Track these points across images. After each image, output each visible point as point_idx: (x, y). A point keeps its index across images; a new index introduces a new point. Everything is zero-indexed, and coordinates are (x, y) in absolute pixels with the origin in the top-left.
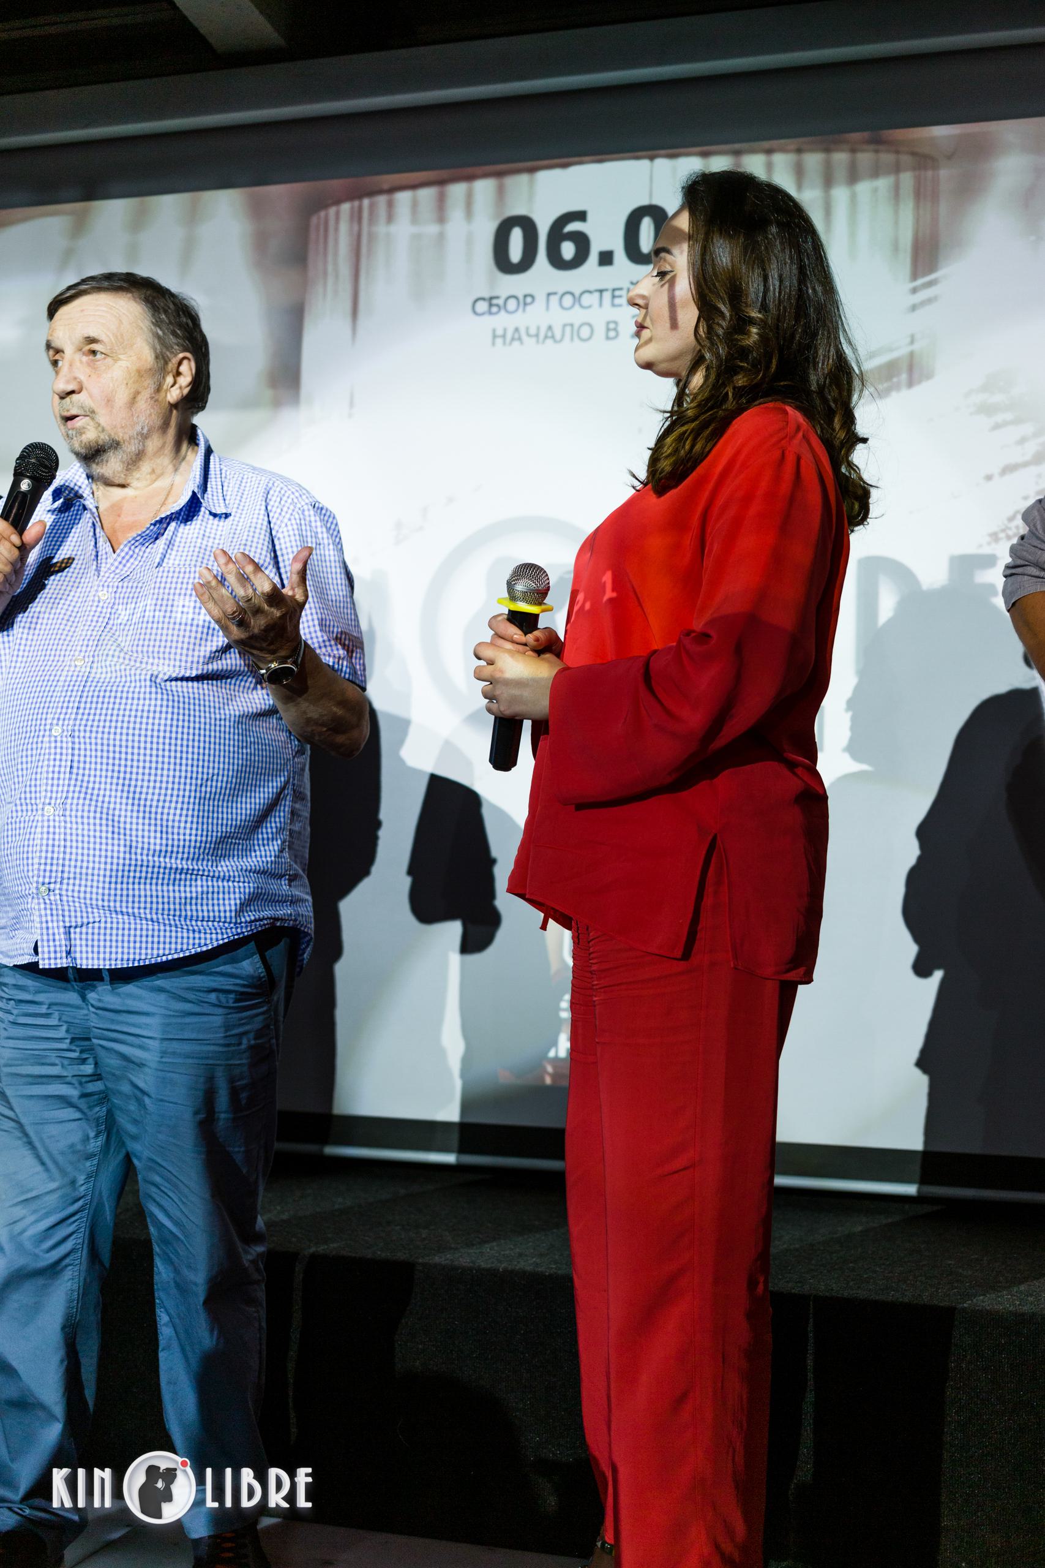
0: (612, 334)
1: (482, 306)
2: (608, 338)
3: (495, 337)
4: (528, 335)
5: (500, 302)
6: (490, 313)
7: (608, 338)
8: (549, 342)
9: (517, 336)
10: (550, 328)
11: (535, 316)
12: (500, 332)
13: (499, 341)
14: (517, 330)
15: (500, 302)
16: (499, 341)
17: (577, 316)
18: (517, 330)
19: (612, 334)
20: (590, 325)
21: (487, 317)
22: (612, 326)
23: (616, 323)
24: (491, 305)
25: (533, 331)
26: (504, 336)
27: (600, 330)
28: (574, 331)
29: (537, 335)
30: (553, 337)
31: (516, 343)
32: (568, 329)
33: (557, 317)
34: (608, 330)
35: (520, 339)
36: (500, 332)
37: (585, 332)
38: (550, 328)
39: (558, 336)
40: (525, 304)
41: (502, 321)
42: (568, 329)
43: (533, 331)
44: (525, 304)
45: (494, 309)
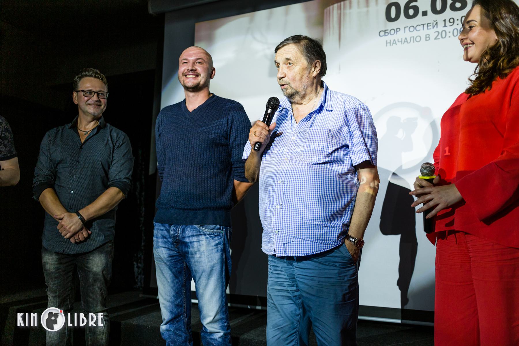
0: (428, 39)
1: (382, 33)
2: (426, 40)
3: (387, 43)
4: (398, 41)
5: (388, 31)
6: (385, 35)
7: (426, 40)
8: (406, 43)
9: (395, 42)
10: (406, 38)
11: (401, 35)
12: (389, 41)
13: (388, 44)
14: (394, 40)
15: (388, 31)
16: (388, 44)
17: (415, 34)
18: (394, 40)
19: (428, 39)
20: (420, 36)
21: (384, 37)
22: (428, 36)
23: (429, 35)
24: (385, 33)
25: (400, 40)
26: (390, 43)
27: (423, 38)
28: (414, 39)
29: (402, 41)
30: (407, 41)
31: (394, 45)
32: (412, 38)
33: (408, 35)
34: (426, 37)
35: (396, 43)
36: (389, 41)
37: (418, 39)
38: (406, 38)
39: (409, 41)
40: (397, 31)
41: (389, 38)
42: (412, 38)
43: (400, 40)
44: (397, 31)
45: (386, 34)
